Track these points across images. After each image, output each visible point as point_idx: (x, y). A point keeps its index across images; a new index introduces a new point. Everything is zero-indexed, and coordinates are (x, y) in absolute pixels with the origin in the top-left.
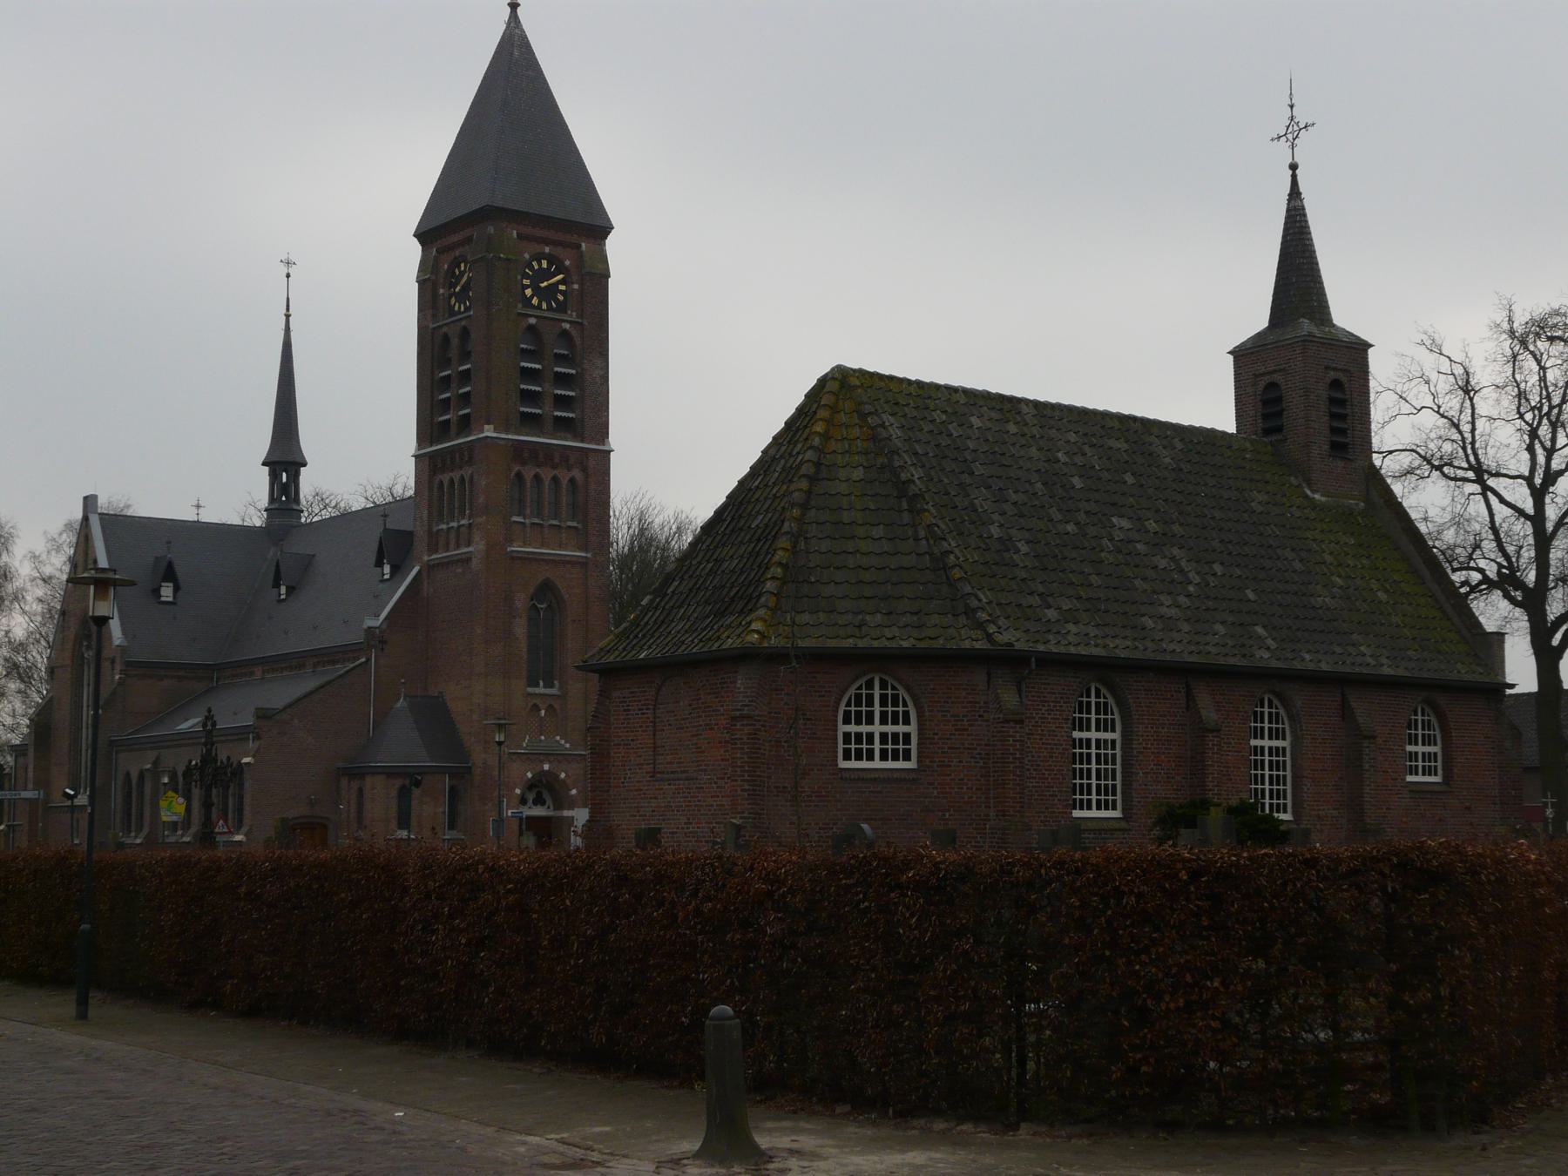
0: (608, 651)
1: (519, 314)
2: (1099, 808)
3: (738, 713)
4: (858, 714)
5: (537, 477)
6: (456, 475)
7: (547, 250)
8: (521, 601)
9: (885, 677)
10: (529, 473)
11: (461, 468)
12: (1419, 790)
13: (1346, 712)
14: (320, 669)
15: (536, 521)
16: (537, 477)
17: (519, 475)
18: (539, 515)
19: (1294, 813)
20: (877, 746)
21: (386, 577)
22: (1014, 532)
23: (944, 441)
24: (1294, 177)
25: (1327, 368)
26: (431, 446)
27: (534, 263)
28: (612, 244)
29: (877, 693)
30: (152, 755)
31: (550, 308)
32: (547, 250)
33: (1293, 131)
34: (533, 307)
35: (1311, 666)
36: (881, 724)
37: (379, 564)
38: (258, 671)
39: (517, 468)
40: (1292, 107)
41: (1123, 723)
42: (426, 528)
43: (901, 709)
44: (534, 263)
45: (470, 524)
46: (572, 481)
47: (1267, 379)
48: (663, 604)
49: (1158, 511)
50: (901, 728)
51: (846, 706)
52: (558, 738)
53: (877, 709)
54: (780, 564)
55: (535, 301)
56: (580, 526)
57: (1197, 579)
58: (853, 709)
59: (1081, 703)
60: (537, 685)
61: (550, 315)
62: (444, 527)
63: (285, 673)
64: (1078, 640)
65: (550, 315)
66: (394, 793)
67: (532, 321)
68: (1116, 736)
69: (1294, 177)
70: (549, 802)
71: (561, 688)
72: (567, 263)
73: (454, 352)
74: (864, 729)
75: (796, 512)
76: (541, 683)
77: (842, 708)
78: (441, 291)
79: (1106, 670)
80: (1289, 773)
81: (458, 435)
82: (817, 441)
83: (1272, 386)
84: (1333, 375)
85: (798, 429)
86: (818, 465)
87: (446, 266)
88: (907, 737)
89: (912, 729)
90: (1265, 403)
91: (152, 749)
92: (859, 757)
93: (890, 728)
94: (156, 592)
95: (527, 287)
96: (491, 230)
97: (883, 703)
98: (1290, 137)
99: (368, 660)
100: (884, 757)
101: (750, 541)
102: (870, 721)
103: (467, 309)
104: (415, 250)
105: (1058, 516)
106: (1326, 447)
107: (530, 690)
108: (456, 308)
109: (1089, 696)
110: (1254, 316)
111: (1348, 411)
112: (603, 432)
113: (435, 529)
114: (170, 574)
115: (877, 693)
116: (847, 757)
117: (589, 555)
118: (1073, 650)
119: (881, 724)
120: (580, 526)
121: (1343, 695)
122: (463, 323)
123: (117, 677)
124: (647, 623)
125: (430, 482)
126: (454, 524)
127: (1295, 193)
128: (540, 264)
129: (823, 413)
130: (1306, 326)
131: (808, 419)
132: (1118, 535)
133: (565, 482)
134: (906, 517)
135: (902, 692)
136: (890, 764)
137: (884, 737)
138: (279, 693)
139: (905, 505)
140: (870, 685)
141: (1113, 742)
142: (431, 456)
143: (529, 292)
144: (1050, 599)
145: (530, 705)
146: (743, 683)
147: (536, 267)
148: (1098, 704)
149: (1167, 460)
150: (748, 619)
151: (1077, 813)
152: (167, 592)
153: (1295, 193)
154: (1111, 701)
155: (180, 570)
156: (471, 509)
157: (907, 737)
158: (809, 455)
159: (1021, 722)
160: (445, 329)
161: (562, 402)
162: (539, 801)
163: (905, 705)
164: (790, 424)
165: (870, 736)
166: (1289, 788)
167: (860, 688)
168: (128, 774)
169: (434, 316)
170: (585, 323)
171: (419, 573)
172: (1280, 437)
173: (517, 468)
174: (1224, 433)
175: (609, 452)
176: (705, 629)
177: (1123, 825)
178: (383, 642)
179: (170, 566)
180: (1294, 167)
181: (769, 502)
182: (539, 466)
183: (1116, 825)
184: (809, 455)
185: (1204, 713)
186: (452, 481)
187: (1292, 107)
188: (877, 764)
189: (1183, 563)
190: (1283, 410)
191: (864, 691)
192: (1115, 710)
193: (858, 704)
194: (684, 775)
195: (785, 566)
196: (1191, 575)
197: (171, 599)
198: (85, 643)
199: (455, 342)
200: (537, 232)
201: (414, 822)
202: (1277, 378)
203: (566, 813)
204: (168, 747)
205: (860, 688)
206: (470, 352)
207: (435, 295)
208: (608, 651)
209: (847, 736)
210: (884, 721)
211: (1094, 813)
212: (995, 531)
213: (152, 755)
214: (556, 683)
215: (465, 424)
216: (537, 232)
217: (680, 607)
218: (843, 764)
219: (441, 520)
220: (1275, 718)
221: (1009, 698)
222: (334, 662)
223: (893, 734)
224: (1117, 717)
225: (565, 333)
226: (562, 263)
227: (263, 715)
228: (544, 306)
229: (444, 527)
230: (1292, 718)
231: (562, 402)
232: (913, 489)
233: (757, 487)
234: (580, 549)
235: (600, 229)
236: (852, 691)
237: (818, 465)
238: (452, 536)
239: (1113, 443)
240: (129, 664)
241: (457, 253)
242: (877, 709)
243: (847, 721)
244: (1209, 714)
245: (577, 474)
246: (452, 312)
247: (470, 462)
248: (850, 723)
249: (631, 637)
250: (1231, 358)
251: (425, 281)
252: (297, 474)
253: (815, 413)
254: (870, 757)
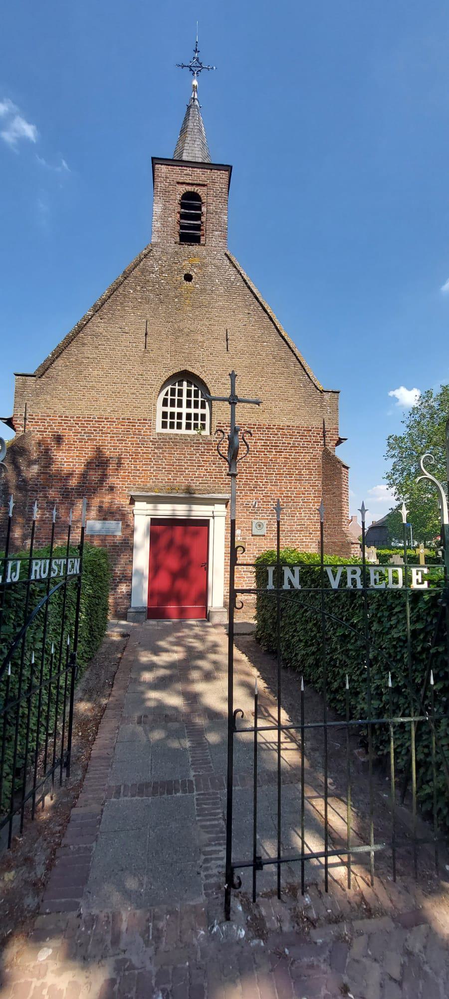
4: (173, 401)
36: (187, 407)
51: (165, 395)
53: (184, 398)
74: (176, 410)
92: (172, 426)
102: (180, 405)
119: (187, 407)
137: (189, 416)
157: (203, 417)
193: (173, 394)
205: (174, 385)
210: (189, 405)
236: (169, 388)
242: (184, 398)
254: (179, 426)
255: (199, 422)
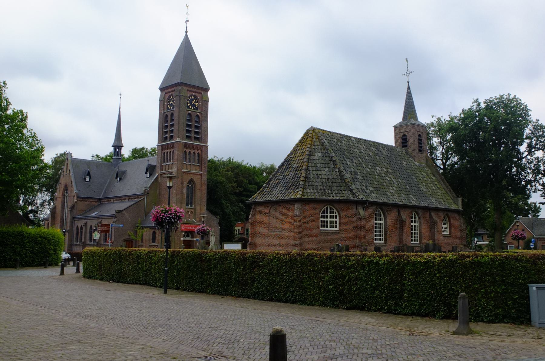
0: (255, 198)
1: (187, 110)
2: (379, 240)
3: (296, 215)
5: (190, 152)
6: (169, 151)
7: (194, 94)
8: (185, 184)
9: (331, 206)
10: (188, 151)
11: (170, 149)
12: (445, 236)
13: (431, 217)
14: (130, 200)
15: (189, 163)
16: (190, 152)
17: (185, 151)
18: (190, 162)
19: (419, 242)
20: (329, 224)
21: (148, 177)
22: (356, 170)
23: (338, 147)
24: (408, 84)
25: (418, 131)
26: (162, 143)
27: (190, 97)
28: (210, 93)
29: (329, 210)
30: (84, 222)
31: (194, 109)
32: (194, 94)
33: (408, 73)
34: (190, 108)
35: (424, 205)
37: (146, 173)
38: (112, 200)
39: (185, 150)
40: (408, 67)
41: (384, 219)
42: (160, 164)
43: (335, 215)
44: (190, 97)
45: (172, 164)
46: (198, 153)
47: (403, 134)
48: (269, 186)
49: (385, 166)
50: (335, 220)
52: (193, 220)
53: (329, 215)
54: (303, 177)
55: (190, 107)
56: (200, 165)
57: (396, 183)
58: (323, 214)
59: (375, 214)
60: (188, 206)
61: (194, 110)
62: (165, 164)
63: (120, 201)
64: (374, 197)
65: (194, 110)
66: (151, 233)
67: (190, 112)
68: (383, 222)
69: (408, 84)
70: (190, 236)
71: (194, 206)
72: (199, 97)
73: (169, 119)
74: (326, 220)
75: (306, 164)
76: (189, 205)
77: (321, 214)
78: (166, 103)
79: (382, 206)
80: (418, 232)
81: (170, 140)
82: (309, 146)
83: (404, 135)
84: (419, 133)
85: (303, 142)
86: (310, 152)
87: (167, 97)
88: (336, 222)
89: (338, 220)
90: (402, 139)
91: (85, 220)
92: (324, 227)
93: (332, 220)
94: (85, 179)
95: (189, 103)
96: (180, 88)
97: (330, 213)
98: (407, 74)
99: (144, 198)
100: (331, 227)
101: (293, 171)
102: (327, 218)
103: (172, 108)
104: (159, 92)
105: (365, 166)
106: (418, 151)
107: (187, 207)
108: (170, 108)
109: (377, 212)
110: (398, 118)
111: (422, 142)
112: (206, 141)
113: (162, 165)
114: (89, 174)
115: (329, 210)
116: (322, 227)
117: (202, 173)
118: (375, 200)
120: (200, 165)
121: (430, 213)
122: (172, 112)
123: (75, 201)
124: (265, 191)
125: (161, 153)
126: (168, 164)
127: (409, 88)
128: (192, 97)
129: (310, 139)
130: (413, 121)
131: (305, 140)
132: (378, 172)
133: (196, 153)
134: (332, 166)
135: (335, 210)
136: (332, 229)
137: (331, 222)
138: (122, 206)
139: (332, 163)
140: (327, 208)
141: (382, 223)
142: (162, 146)
143: (189, 104)
144: (367, 187)
145: (187, 211)
146: (297, 208)
147: (191, 98)
148: (379, 214)
149: (384, 153)
150: (297, 191)
151: (375, 242)
152: (88, 179)
153: (409, 88)
154: (382, 213)
155: (91, 173)
156: (173, 159)
157: (336, 222)
158: (308, 149)
159: (365, 218)
160: (166, 113)
161: (196, 133)
162: (188, 236)
163: (336, 214)
164: (300, 141)
165: (327, 222)
166: (418, 235)
167: (325, 209)
168: (78, 227)
169: (163, 110)
170: (203, 113)
171: (158, 176)
172: (407, 148)
173: (185, 150)
174: (392, 146)
175: (207, 146)
176: (284, 193)
177: (385, 245)
178: (148, 193)
179: (89, 172)
180: (408, 82)
181: (297, 161)
182: (190, 149)
183: (383, 244)
184: (308, 149)
185: (402, 216)
186: (167, 153)
187: (408, 67)
188: (329, 228)
189: (392, 179)
190: (407, 142)
191: (326, 210)
192: (383, 216)
193: (324, 213)
194: (278, 231)
195: (305, 178)
196: (395, 182)
197: (89, 181)
198: (66, 192)
199: (169, 116)
200: (192, 89)
201: (156, 241)
202: (406, 133)
203: (195, 239)
204: (89, 219)
205: (325, 209)
206: (173, 119)
207: (164, 104)
208: (255, 198)
209: (322, 221)
210: (330, 218)
211: (378, 242)
212: (352, 169)
213: (84, 222)
214: (193, 205)
215: (172, 137)
216: (192, 89)
217: (275, 187)
218: (321, 229)
219: (164, 162)
220: (415, 218)
221: (362, 212)
222: (134, 198)
223: (324, 221)
224: (383, 217)
225: (197, 115)
226: (197, 97)
227: (119, 212)
228: (193, 108)
229: (165, 164)
230: (419, 218)
231: (196, 133)
232: (334, 159)
233: (293, 157)
234: (200, 171)
235: (206, 89)
236: (323, 210)
237: (310, 152)
238: (167, 166)
239: (373, 148)
240: (78, 197)
241: (170, 94)
242: (329, 215)
243: (322, 218)
244: (404, 217)
245: (199, 151)
246: (168, 109)
247: (173, 147)
248: (322, 218)
249: (262, 194)
250: (394, 128)
251: (162, 100)
252: (121, 149)
253: (307, 138)
254: (327, 227)
255: (335, 224)
